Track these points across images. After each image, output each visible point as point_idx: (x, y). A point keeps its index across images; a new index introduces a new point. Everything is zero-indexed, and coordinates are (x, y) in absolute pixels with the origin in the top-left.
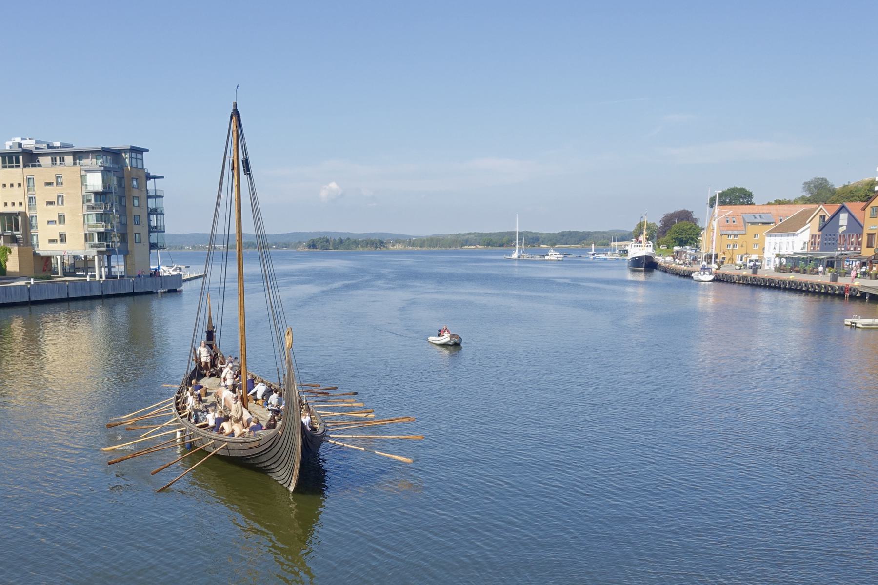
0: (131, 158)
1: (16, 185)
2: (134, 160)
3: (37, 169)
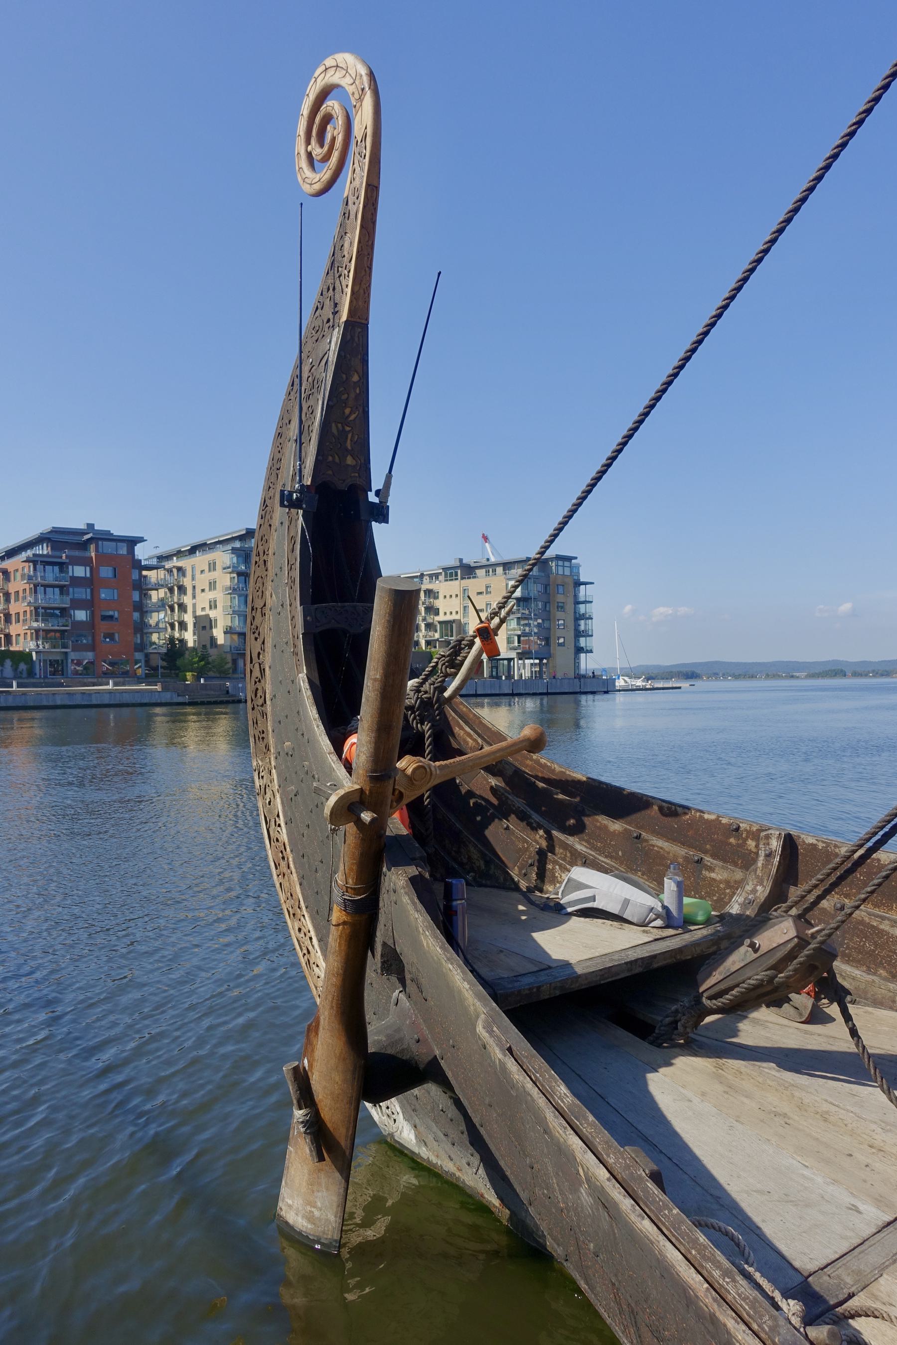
0: (557, 565)
1: (454, 596)
2: (560, 569)
3: (472, 580)
